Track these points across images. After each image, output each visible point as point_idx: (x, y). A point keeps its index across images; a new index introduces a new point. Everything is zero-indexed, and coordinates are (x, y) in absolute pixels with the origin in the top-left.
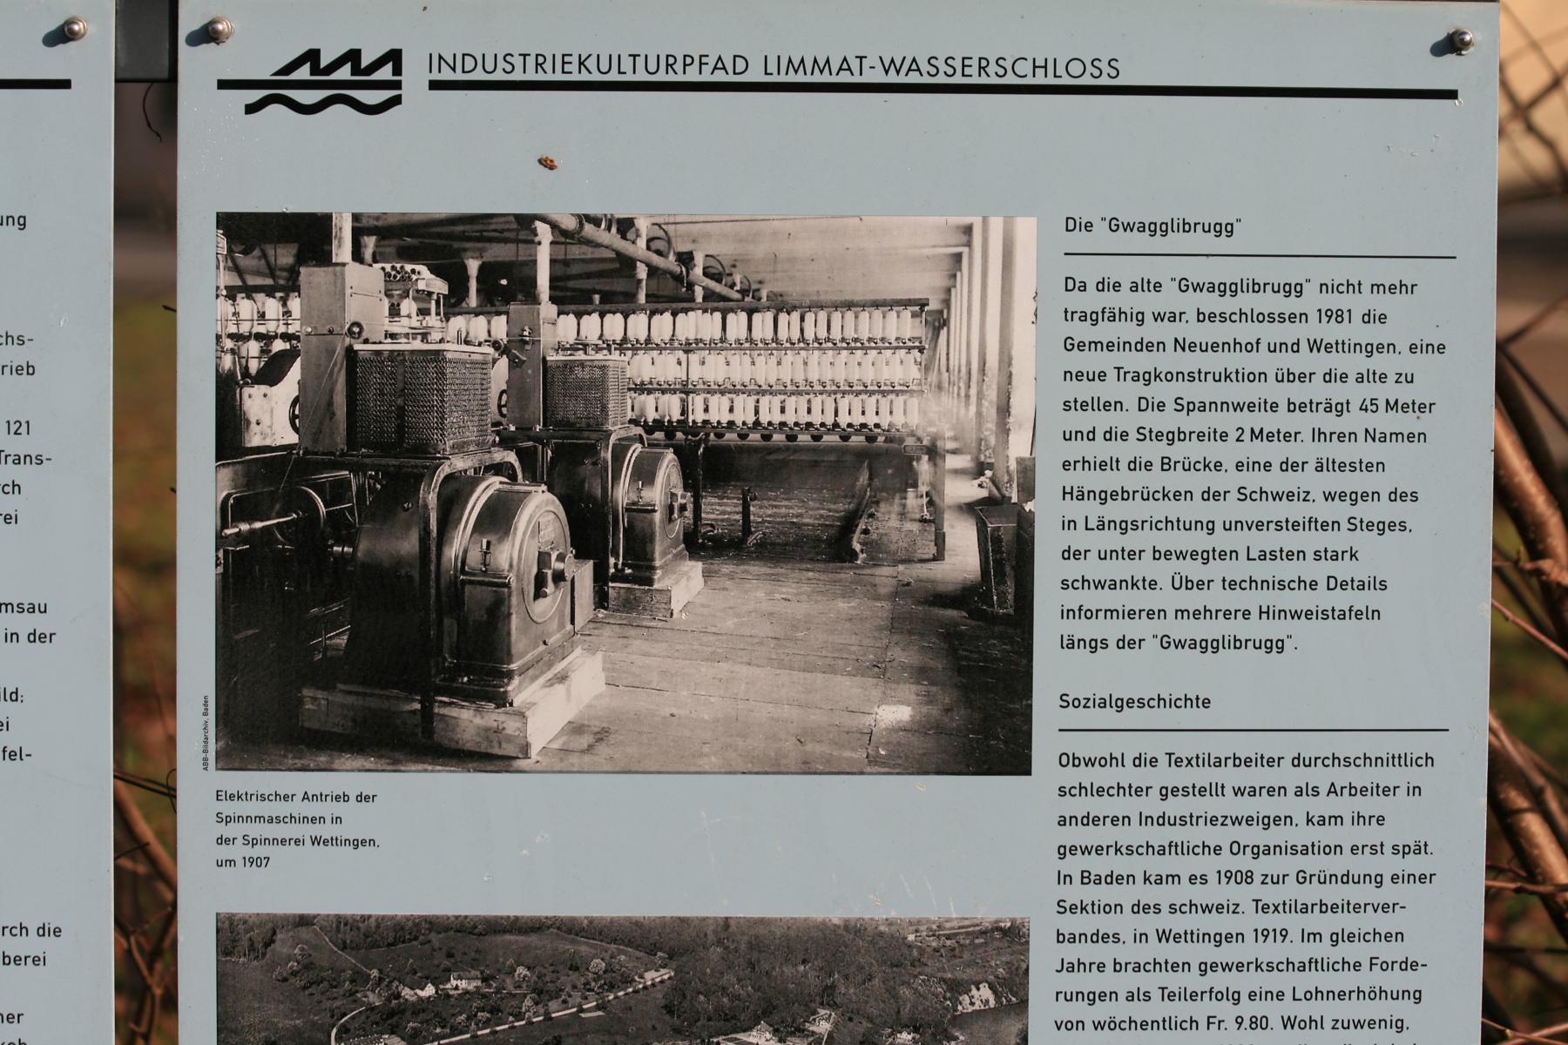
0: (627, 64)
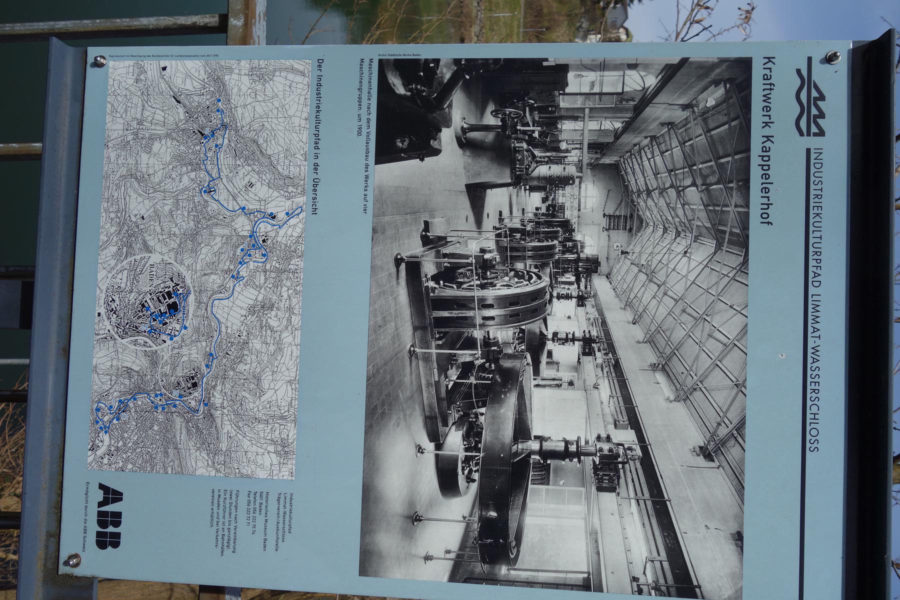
0: (817, 234)
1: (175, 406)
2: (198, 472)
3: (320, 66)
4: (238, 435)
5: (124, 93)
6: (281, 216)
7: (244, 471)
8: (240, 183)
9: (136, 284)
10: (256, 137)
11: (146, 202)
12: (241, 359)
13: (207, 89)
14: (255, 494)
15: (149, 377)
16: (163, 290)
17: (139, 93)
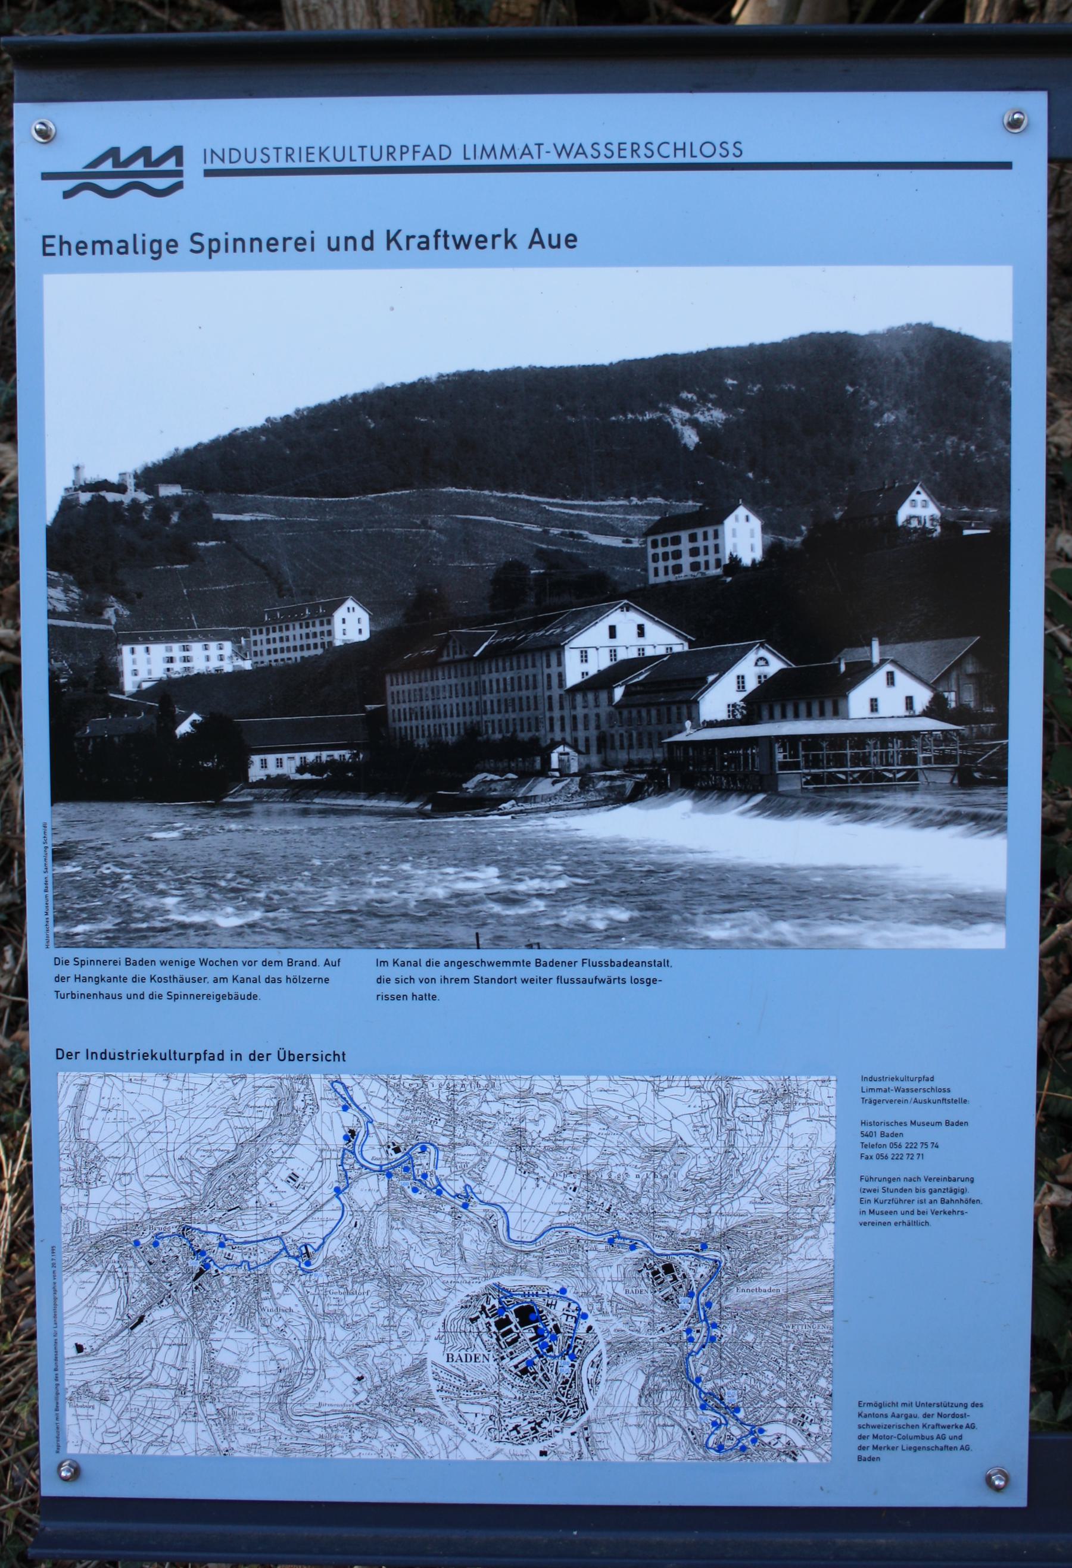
1: (709, 1304)
2: (829, 1254)
3: (69, 1055)
4: (757, 1184)
5: (127, 1423)
6: (349, 1119)
7: (824, 1170)
8: (288, 1198)
9: (484, 1386)
10: (204, 1171)
11: (330, 1373)
12: (618, 1185)
13: (117, 1265)
14: (866, 1146)
15: (656, 1355)
16: (495, 1336)
17: (127, 1394)
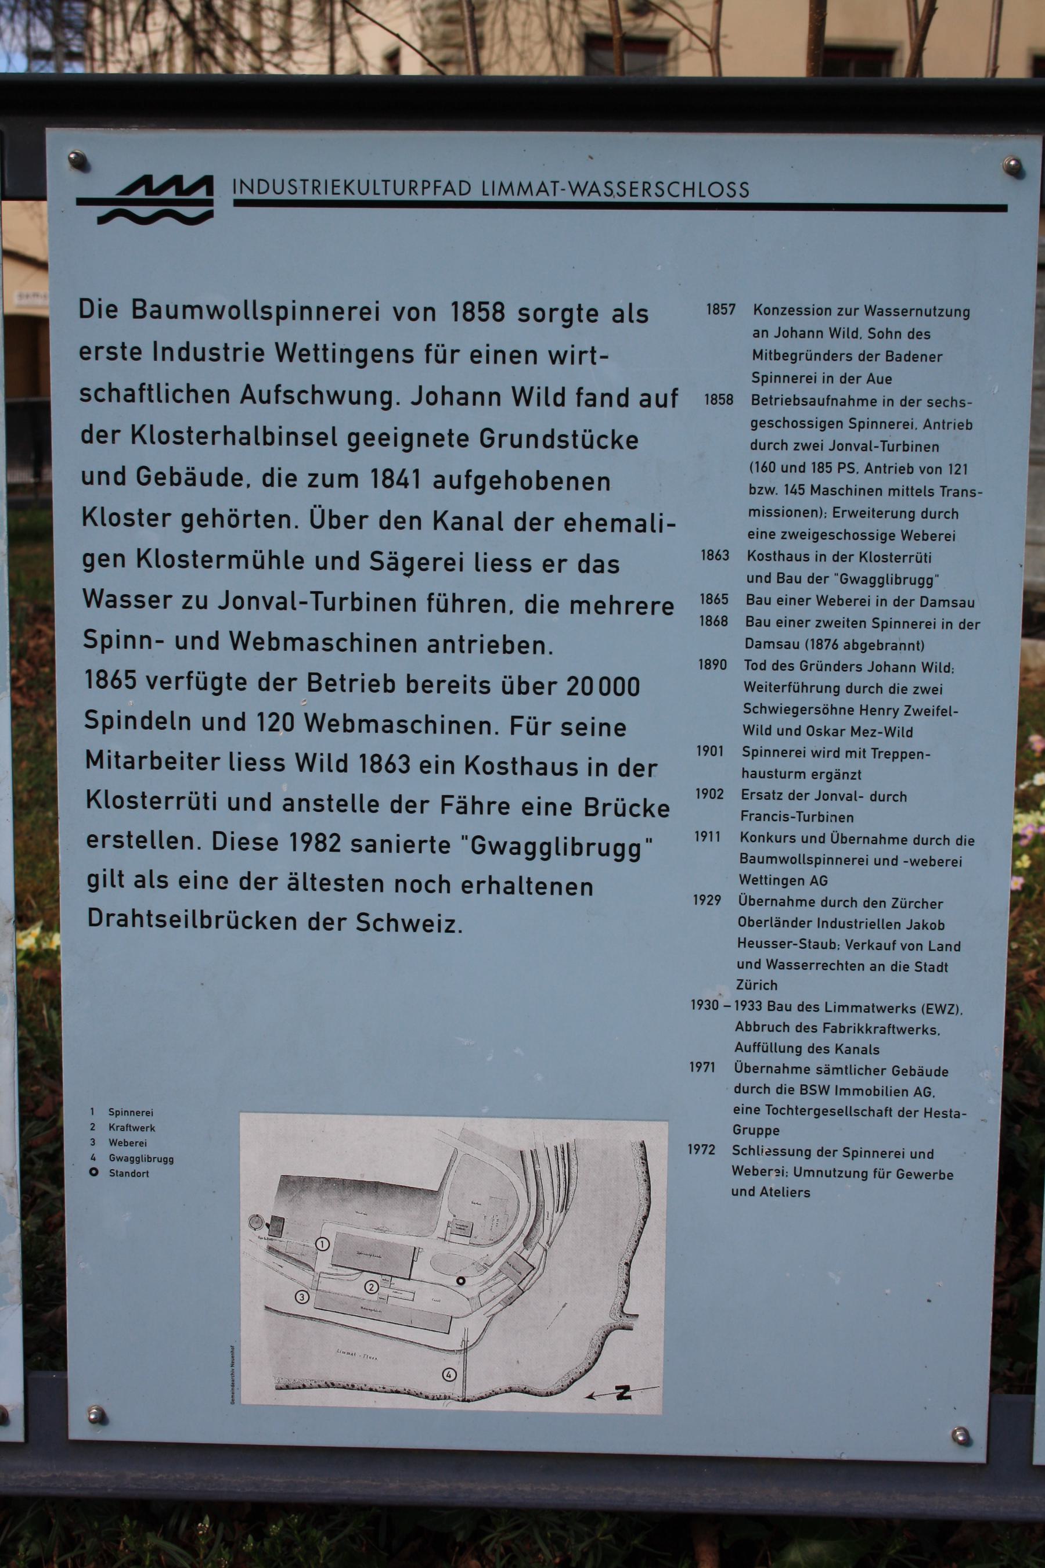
0: (380, 188)
